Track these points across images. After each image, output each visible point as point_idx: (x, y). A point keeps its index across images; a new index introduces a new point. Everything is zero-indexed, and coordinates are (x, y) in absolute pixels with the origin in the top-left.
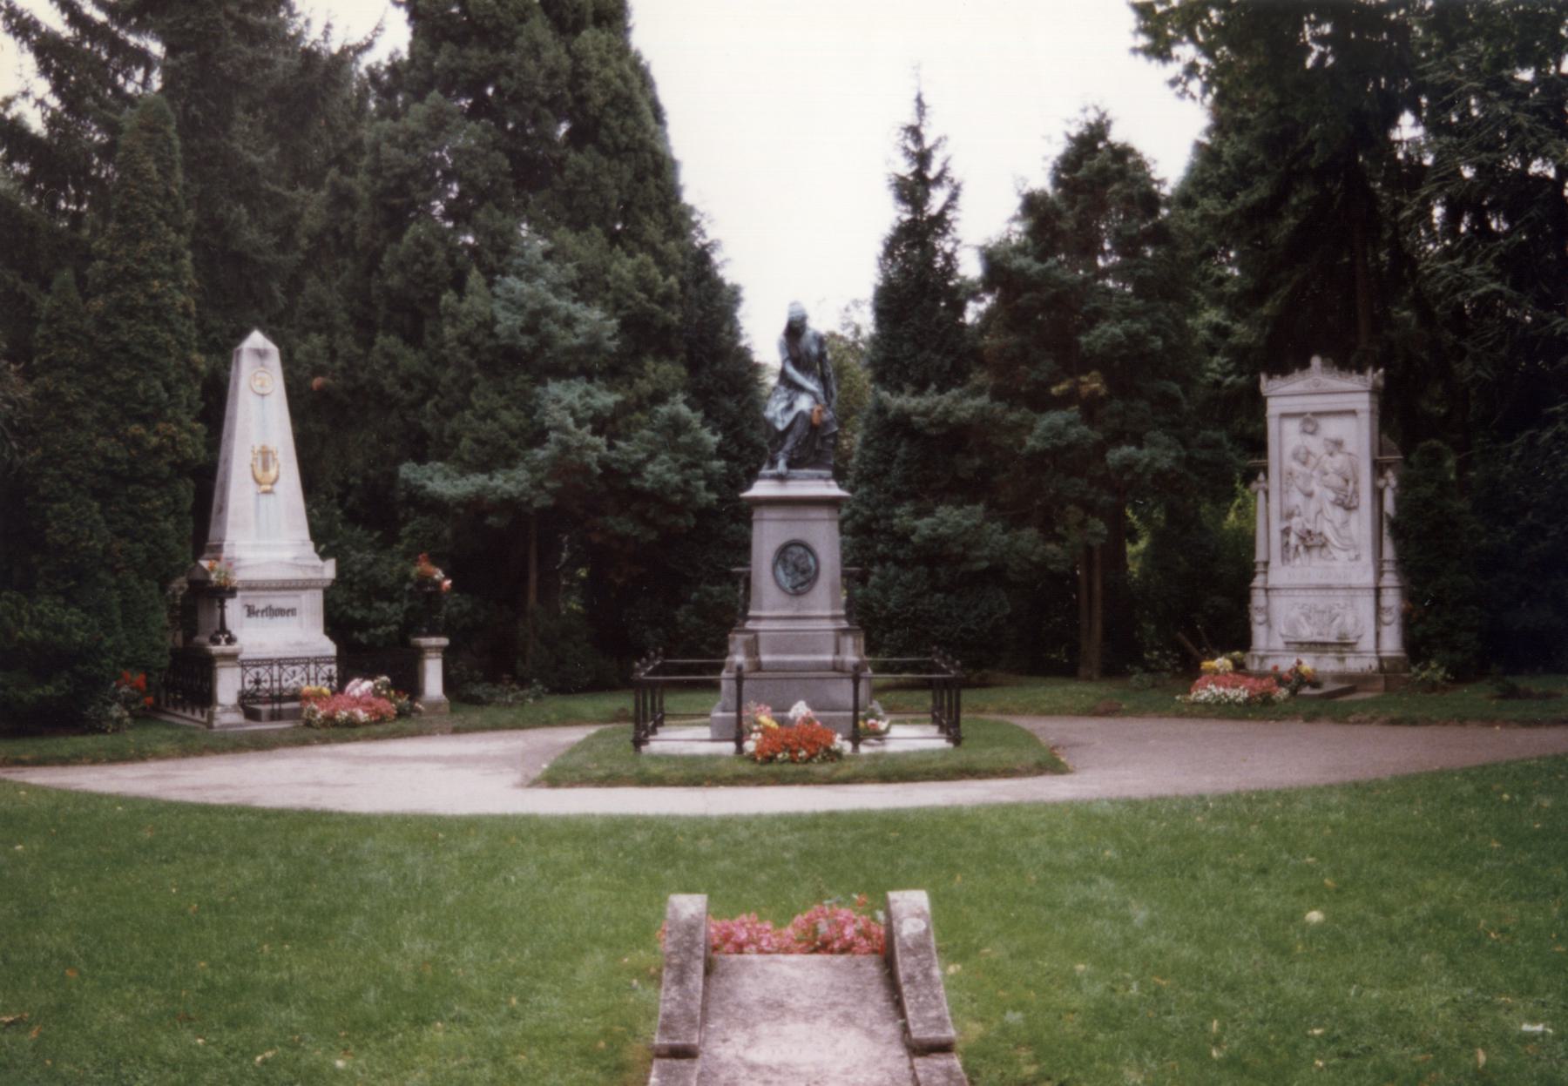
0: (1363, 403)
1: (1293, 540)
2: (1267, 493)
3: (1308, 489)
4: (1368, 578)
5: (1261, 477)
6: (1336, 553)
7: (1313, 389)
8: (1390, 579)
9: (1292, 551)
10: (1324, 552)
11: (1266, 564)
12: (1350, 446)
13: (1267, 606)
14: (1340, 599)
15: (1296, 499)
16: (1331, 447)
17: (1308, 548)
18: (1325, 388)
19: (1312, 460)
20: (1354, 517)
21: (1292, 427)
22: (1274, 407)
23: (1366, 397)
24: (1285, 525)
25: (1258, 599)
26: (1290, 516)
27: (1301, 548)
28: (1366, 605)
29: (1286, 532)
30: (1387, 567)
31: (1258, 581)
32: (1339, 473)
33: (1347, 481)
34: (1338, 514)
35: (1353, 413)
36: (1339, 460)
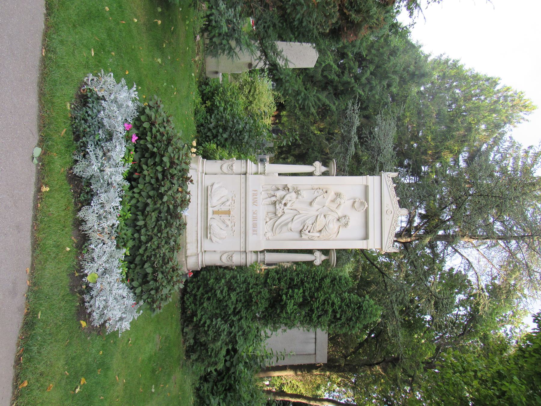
0: (372, 245)
1: (280, 194)
3: (315, 204)
5: (324, 169)
6: (271, 223)
7: (385, 209)
8: (251, 259)
9: (273, 193)
10: (271, 215)
12: (343, 233)
17: (274, 203)
18: (385, 216)
19: (333, 206)
20: (297, 236)
21: (359, 194)
22: (372, 181)
25: (238, 165)
26: (297, 192)
27: (274, 199)
28: (235, 245)
29: (286, 188)
30: (260, 257)
31: (251, 167)
33: (320, 231)
34: (296, 225)
35: (366, 237)
36: (333, 226)
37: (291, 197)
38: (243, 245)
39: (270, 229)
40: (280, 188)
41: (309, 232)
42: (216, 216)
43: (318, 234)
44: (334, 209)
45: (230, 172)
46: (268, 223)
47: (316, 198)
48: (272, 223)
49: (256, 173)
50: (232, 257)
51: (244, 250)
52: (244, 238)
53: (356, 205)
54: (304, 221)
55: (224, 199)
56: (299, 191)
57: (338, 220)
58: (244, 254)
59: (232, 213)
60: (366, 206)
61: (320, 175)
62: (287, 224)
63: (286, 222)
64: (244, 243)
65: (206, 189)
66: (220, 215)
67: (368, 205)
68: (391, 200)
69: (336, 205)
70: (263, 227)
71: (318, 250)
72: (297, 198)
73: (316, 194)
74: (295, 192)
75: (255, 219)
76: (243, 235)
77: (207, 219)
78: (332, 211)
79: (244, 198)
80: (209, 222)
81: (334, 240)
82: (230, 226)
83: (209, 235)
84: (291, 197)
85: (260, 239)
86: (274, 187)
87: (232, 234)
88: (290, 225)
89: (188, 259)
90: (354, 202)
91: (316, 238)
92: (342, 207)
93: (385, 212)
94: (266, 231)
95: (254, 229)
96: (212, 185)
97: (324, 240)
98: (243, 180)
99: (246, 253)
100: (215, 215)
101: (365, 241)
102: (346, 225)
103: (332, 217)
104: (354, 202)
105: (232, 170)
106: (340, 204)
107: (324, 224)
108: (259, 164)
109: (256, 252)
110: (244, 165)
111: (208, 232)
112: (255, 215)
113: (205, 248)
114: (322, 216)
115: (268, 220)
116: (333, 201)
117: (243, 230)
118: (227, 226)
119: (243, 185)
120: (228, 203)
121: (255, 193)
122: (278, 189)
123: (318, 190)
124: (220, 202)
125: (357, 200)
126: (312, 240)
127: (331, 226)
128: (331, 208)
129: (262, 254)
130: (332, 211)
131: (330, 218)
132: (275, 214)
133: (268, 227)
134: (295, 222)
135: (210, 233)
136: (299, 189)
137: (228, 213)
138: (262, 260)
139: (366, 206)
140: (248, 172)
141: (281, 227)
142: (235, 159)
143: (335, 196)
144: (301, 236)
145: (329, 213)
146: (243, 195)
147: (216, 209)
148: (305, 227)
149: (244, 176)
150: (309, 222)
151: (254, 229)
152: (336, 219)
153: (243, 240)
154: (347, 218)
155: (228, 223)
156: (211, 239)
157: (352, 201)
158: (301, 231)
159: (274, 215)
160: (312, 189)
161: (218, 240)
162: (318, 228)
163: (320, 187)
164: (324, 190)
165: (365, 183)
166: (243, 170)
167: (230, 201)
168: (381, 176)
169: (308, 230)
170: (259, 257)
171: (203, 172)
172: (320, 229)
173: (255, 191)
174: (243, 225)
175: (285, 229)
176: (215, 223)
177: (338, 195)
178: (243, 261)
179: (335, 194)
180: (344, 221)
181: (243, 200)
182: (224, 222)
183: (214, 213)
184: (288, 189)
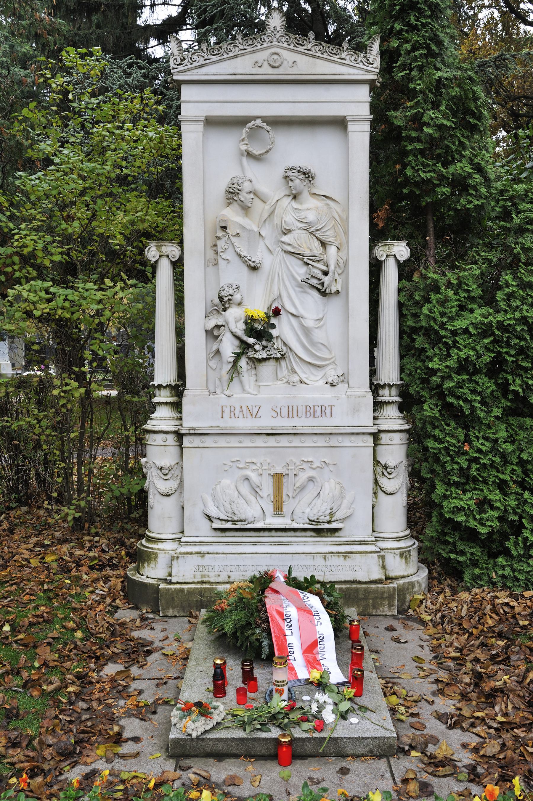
2: (178, 265)
4: (365, 419)
6: (303, 373)
7: (266, 72)
8: (393, 418)
11: (178, 389)
13: (180, 464)
14: (312, 451)
15: (232, 274)
16: (298, 183)
21: (228, 143)
23: (363, 94)
24: (211, 324)
25: (159, 454)
29: (213, 334)
31: (162, 418)
32: (310, 230)
33: (323, 244)
35: (340, 123)
37: (236, 322)
38: (359, 441)
39: (320, 373)
40: (215, 348)
41: (326, 273)
42: (287, 509)
43: (332, 250)
44: (267, 207)
45: (176, 472)
46: (303, 377)
47: (240, 256)
48: (305, 368)
49: (177, 406)
50: (385, 467)
51: (370, 441)
52: (340, 438)
53: (256, 151)
54: (300, 286)
55: (245, 489)
56: (221, 298)
57: (295, 197)
58: (383, 436)
59: (279, 470)
60: (259, 122)
61: (181, 243)
62: (307, 331)
63: (299, 333)
64: (353, 438)
65: (219, 534)
66: (285, 498)
67: (255, 118)
68: (243, 55)
69: (257, 201)
70: (314, 389)
71: (371, 249)
72: (239, 304)
73: (229, 255)
74: (225, 310)
75: (291, 412)
76: (334, 441)
77: (295, 530)
78: (272, 213)
79: (241, 438)
80: (301, 526)
81: (347, 209)
82: (311, 473)
83: (334, 525)
84: (236, 322)
85: (352, 407)
86: (213, 363)
87: (331, 468)
88: (309, 323)
89: (392, 574)
90: (249, 154)
91: (342, 254)
92: (263, 188)
93: (275, 71)
94: (322, 382)
95: (318, 413)
96: (209, 518)
97: (346, 232)
98: (197, 441)
99: (380, 431)
100: (285, 509)
101: (351, 127)
102: (308, 175)
103: (288, 213)
104: (249, 154)
105: (170, 469)
106: (255, 194)
107: (304, 235)
108: (155, 400)
109: (378, 405)
110: (159, 439)
111: (327, 526)
112: (285, 412)
113: (365, 533)
114: (285, 239)
115: (295, 378)
116: (246, 209)
117: (321, 441)
118: (311, 479)
119: (208, 441)
120: (254, 476)
121: (227, 411)
122: (218, 352)
123: (219, 250)
124: (252, 498)
125: (244, 148)
126: (346, 263)
127: (311, 217)
128: (265, 215)
129: (381, 392)
130: (272, 213)
131: (290, 219)
132: (277, 359)
133: (315, 379)
134: (302, 311)
135: (329, 522)
136: (217, 301)
137: (278, 479)
138: (394, 391)
139: (259, 122)
140: (173, 429)
141: (313, 343)
142: (143, 460)
143: (235, 206)
144: (338, 292)
145: (277, 221)
146: (233, 442)
147: (270, 509)
148: (314, 282)
149: (186, 441)
150: (301, 272)
151: (318, 413)
152: (294, 204)
153: (346, 441)
154: (290, 173)
155: (303, 477)
156: (343, 520)
157: (244, 159)
158: (324, 294)
159: (283, 363)
160: (216, 264)
161: (345, 501)
162: (317, 249)
163: (209, 244)
164: (220, 233)
165: (200, 126)
166: (171, 439)
167: (249, 473)
168: (179, 83)
169: (320, 275)
170: (387, 399)
171: (178, 540)
172: (317, 244)
173: (223, 412)
174: (309, 441)
175: (319, 336)
176: (303, 509)
177: (232, 194)
178: (397, 438)
179: (229, 204)
180: (297, 181)
181: (247, 442)
182: (302, 488)
183: (278, 511)
184: (218, 327)
